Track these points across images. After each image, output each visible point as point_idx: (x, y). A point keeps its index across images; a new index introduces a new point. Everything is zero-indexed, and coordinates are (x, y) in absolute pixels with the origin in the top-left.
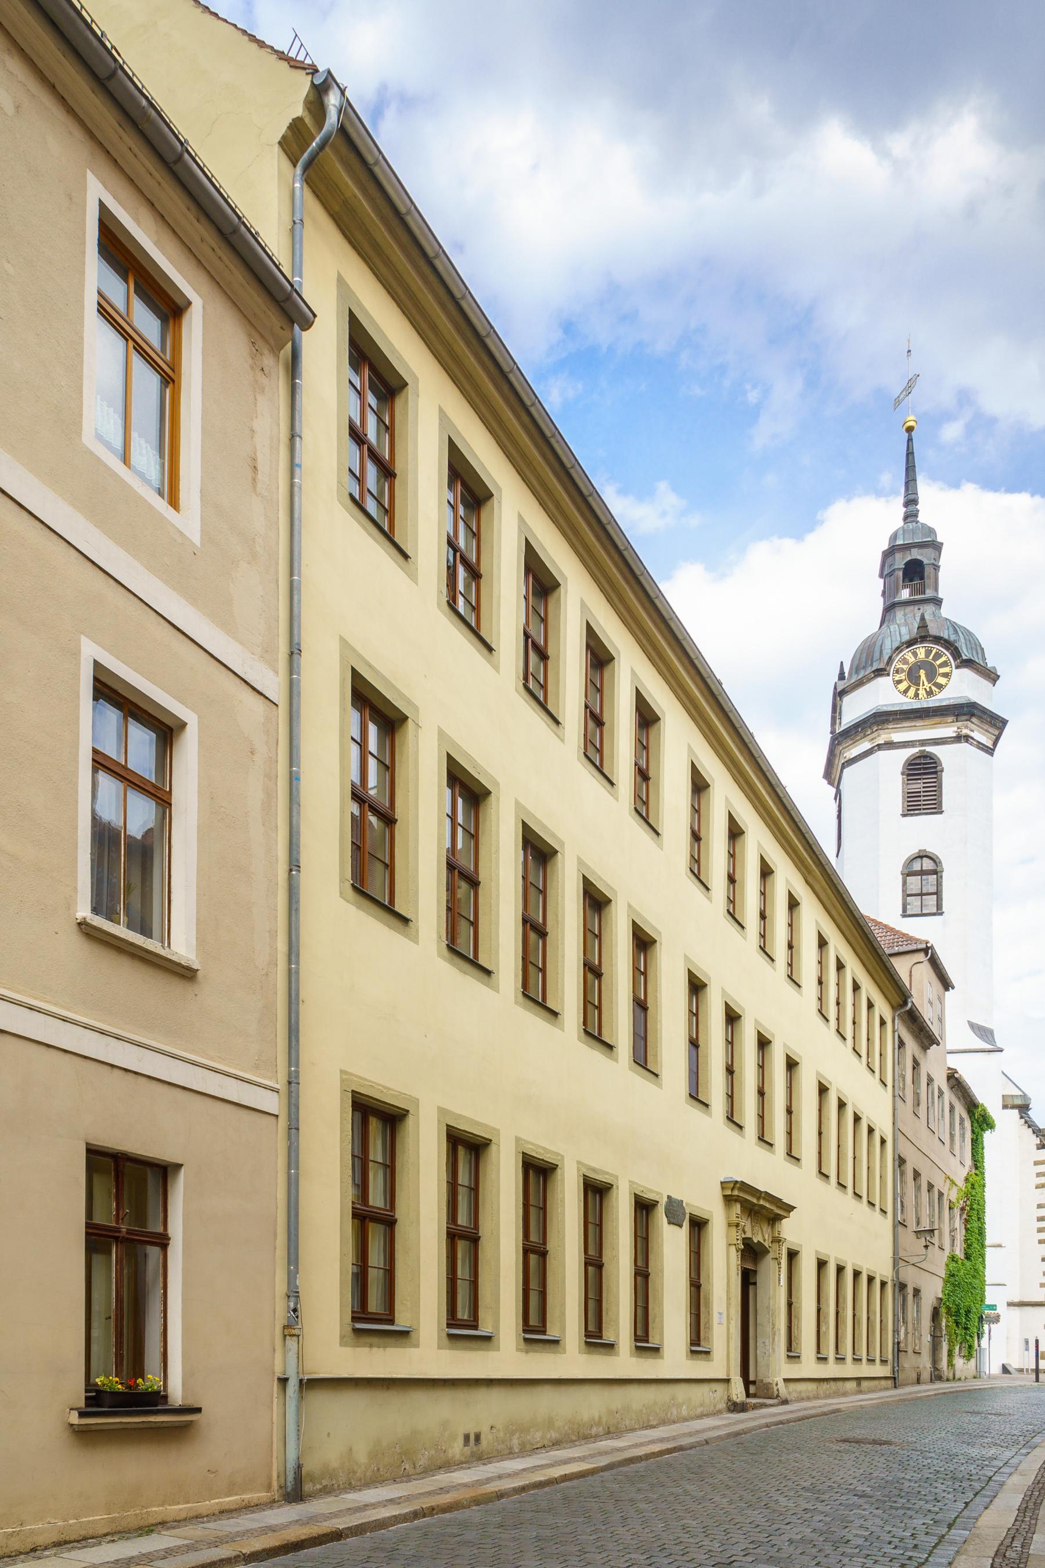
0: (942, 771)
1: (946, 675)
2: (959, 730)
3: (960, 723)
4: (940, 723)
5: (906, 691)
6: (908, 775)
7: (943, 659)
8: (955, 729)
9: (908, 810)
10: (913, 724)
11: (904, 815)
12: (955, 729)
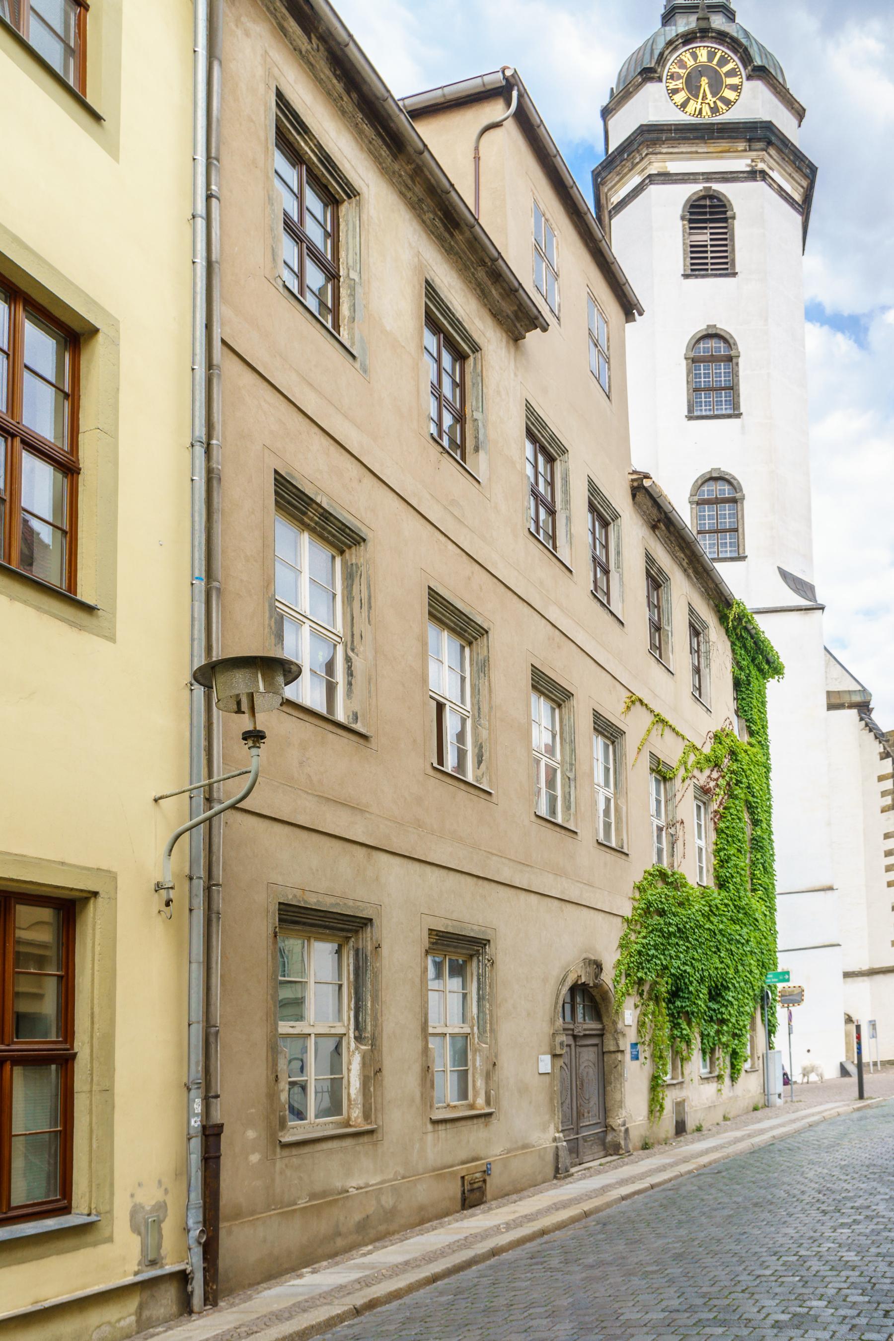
0: (734, 218)
1: (735, 88)
2: (754, 164)
3: (755, 153)
4: (728, 151)
5: (684, 105)
6: (691, 221)
7: (730, 66)
8: (749, 161)
9: (692, 270)
10: (694, 149)
11: (686, 276)
12: (749, 161)
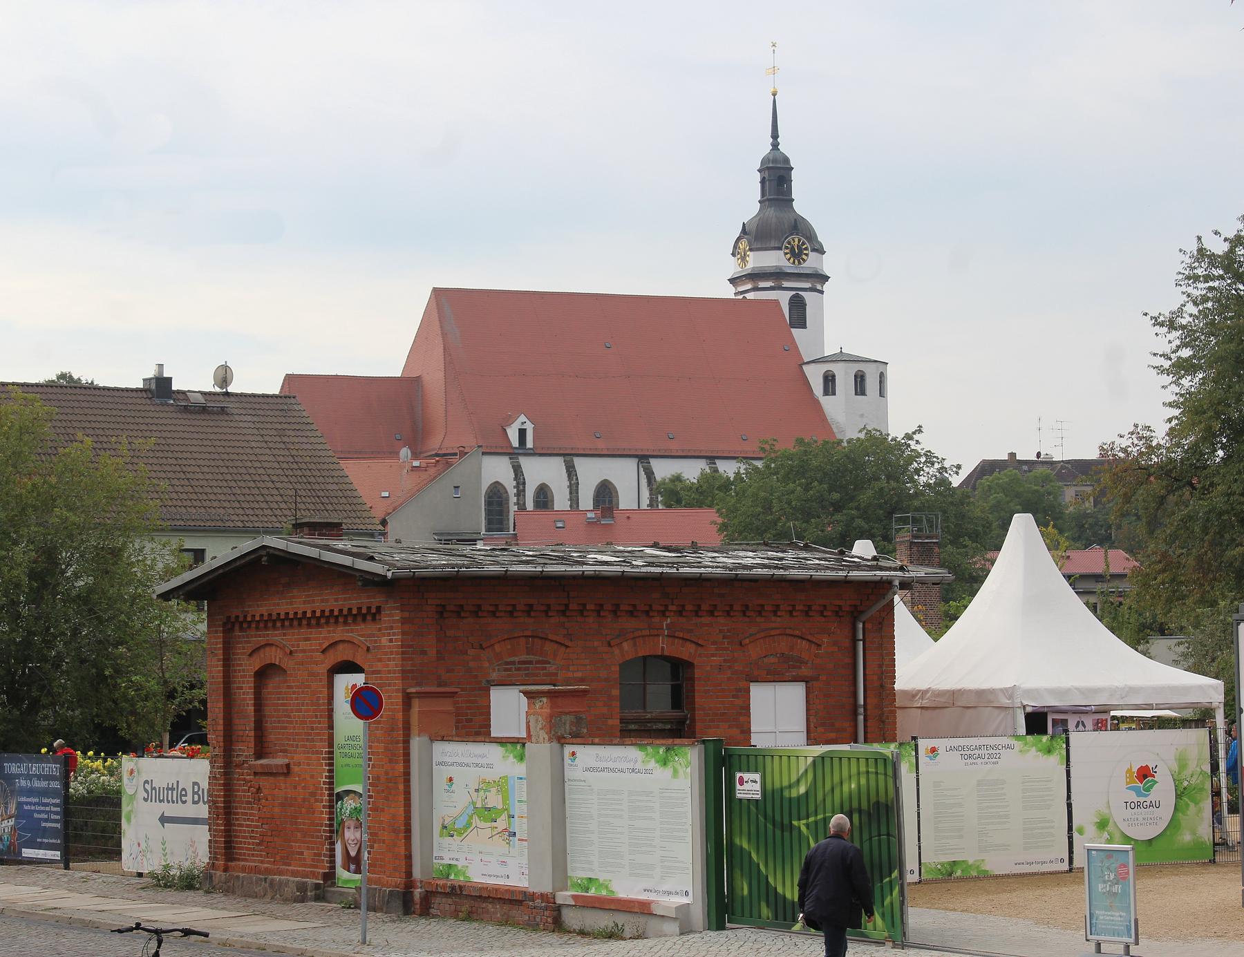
5: (789, 260)
7: (805, 246)
